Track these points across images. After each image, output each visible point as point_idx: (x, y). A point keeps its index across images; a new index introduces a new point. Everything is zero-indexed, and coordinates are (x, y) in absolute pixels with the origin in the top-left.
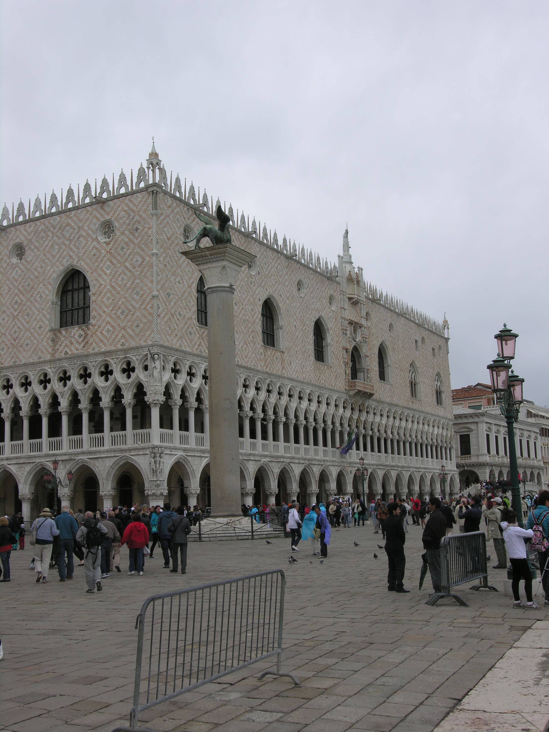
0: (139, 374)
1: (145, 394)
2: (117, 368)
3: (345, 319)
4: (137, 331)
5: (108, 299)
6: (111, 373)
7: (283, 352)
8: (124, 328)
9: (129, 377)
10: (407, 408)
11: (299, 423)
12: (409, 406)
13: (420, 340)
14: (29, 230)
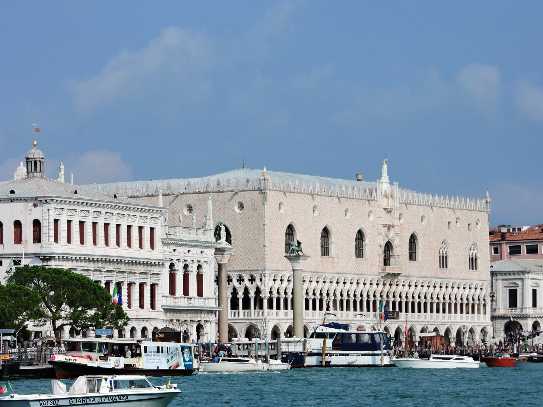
0: (258, 282)
1: (260, 293)
2: (246, 278)
3: (380, 224)
4: (257, 261)
5: (241, 243)
6: (243, 280)
7: (334, 258)
8: (250, 259)
9: (252, 283)
10: (434, 278)
11: (343, 298)
12: (438, 276)
13: (453, 221)
14: (195, 198)
